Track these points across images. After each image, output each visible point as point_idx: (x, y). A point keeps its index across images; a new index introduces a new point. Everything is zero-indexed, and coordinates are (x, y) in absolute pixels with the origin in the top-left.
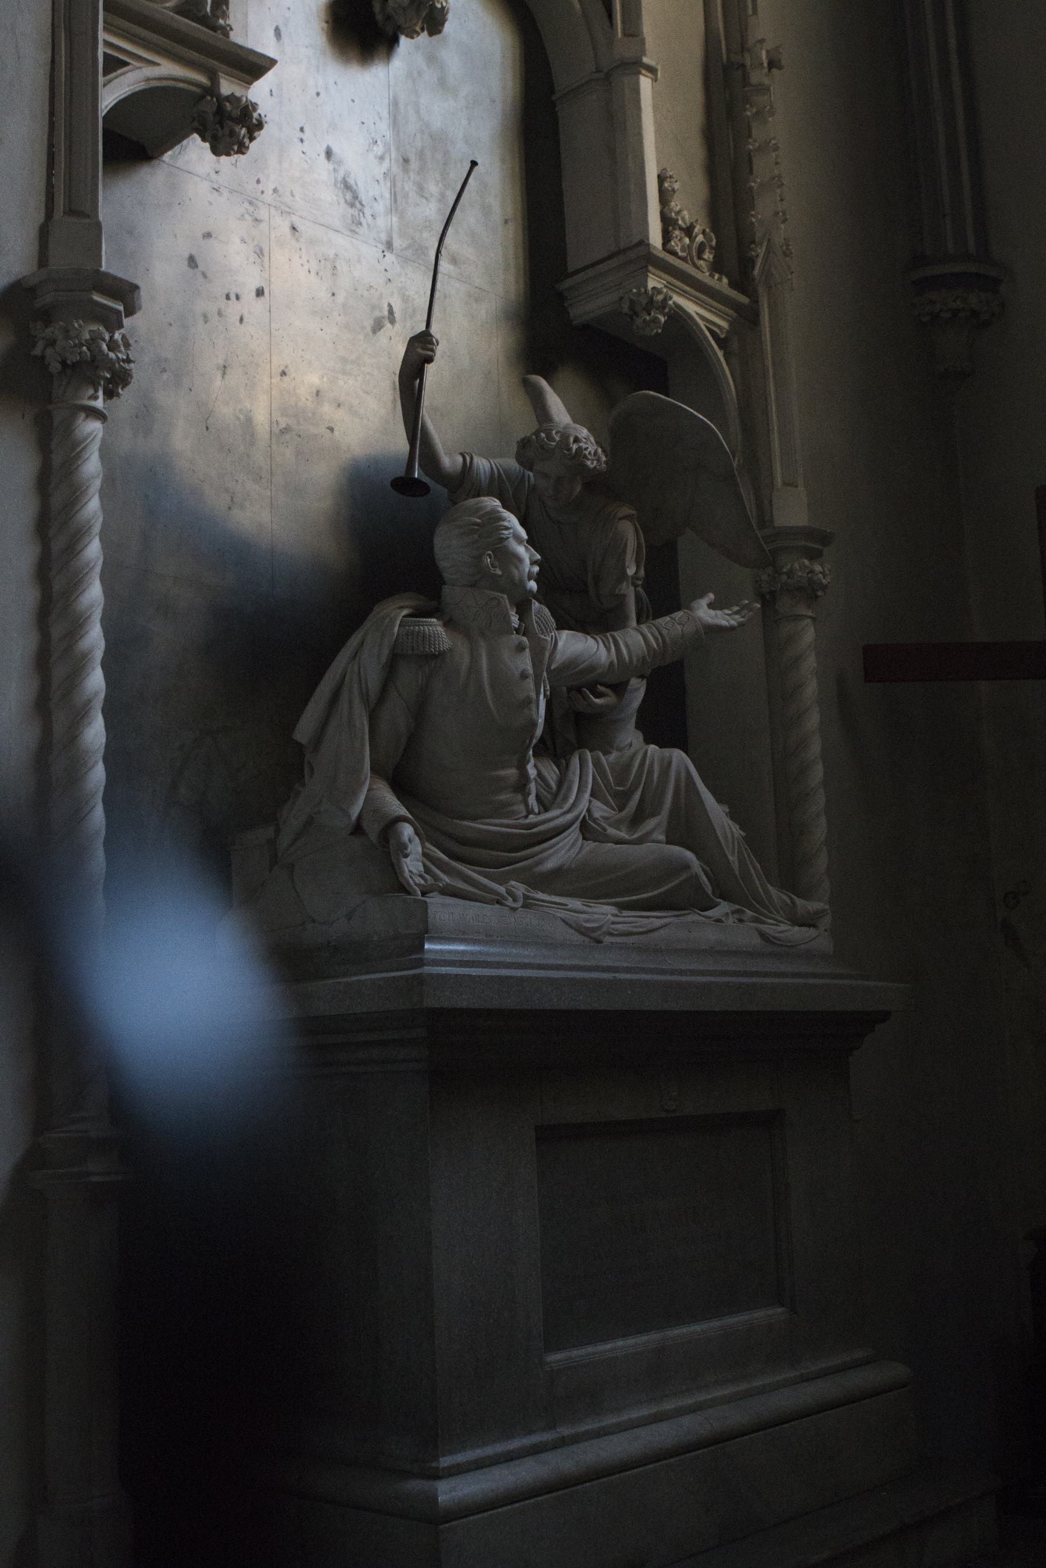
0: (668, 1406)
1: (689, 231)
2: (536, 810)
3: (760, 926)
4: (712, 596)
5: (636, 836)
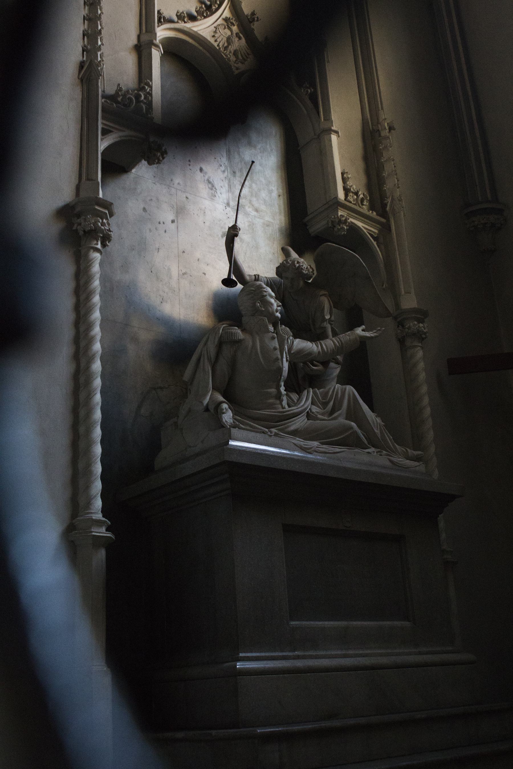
0: (351, 652)
1: (356, 194)
3: (390, 458)
4: (364, 327)
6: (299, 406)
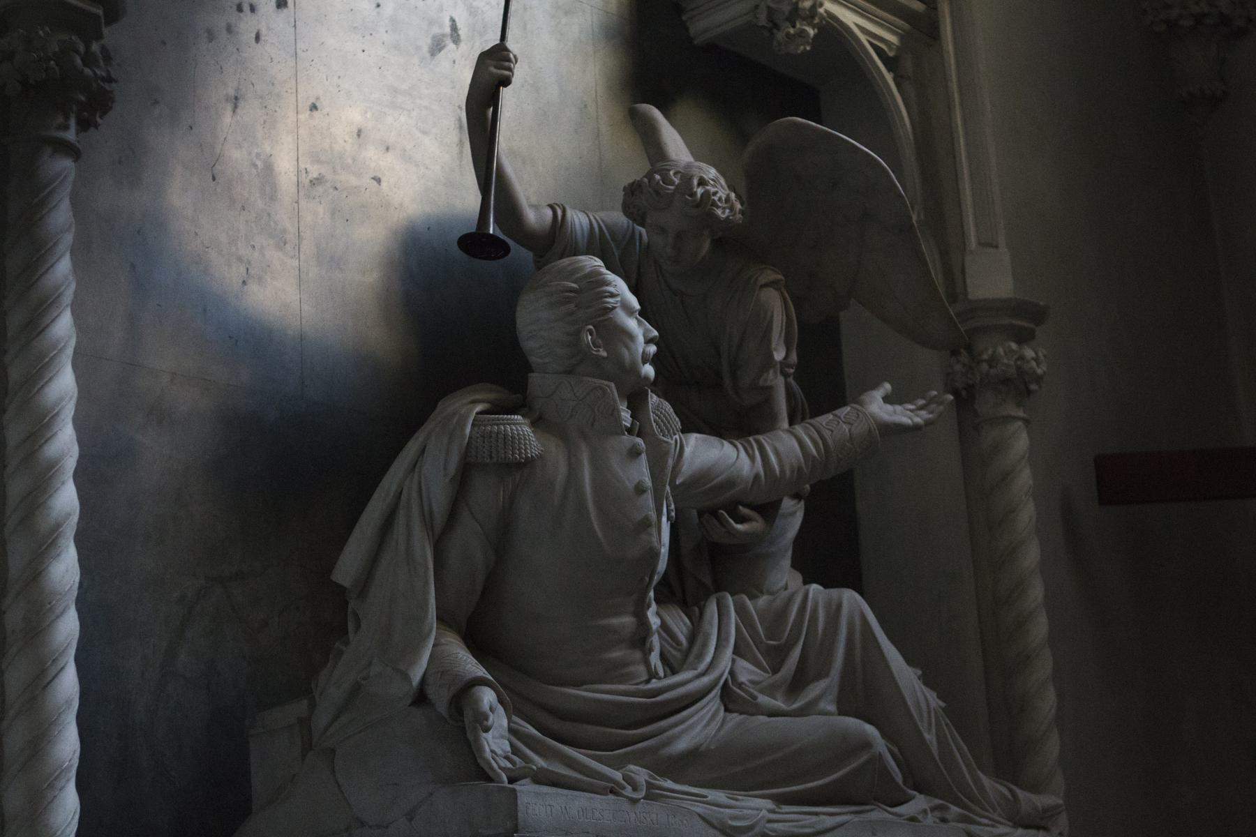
2: (661, 674)
3: (973, 828)
4: (888, 386)
5: (795, 706)
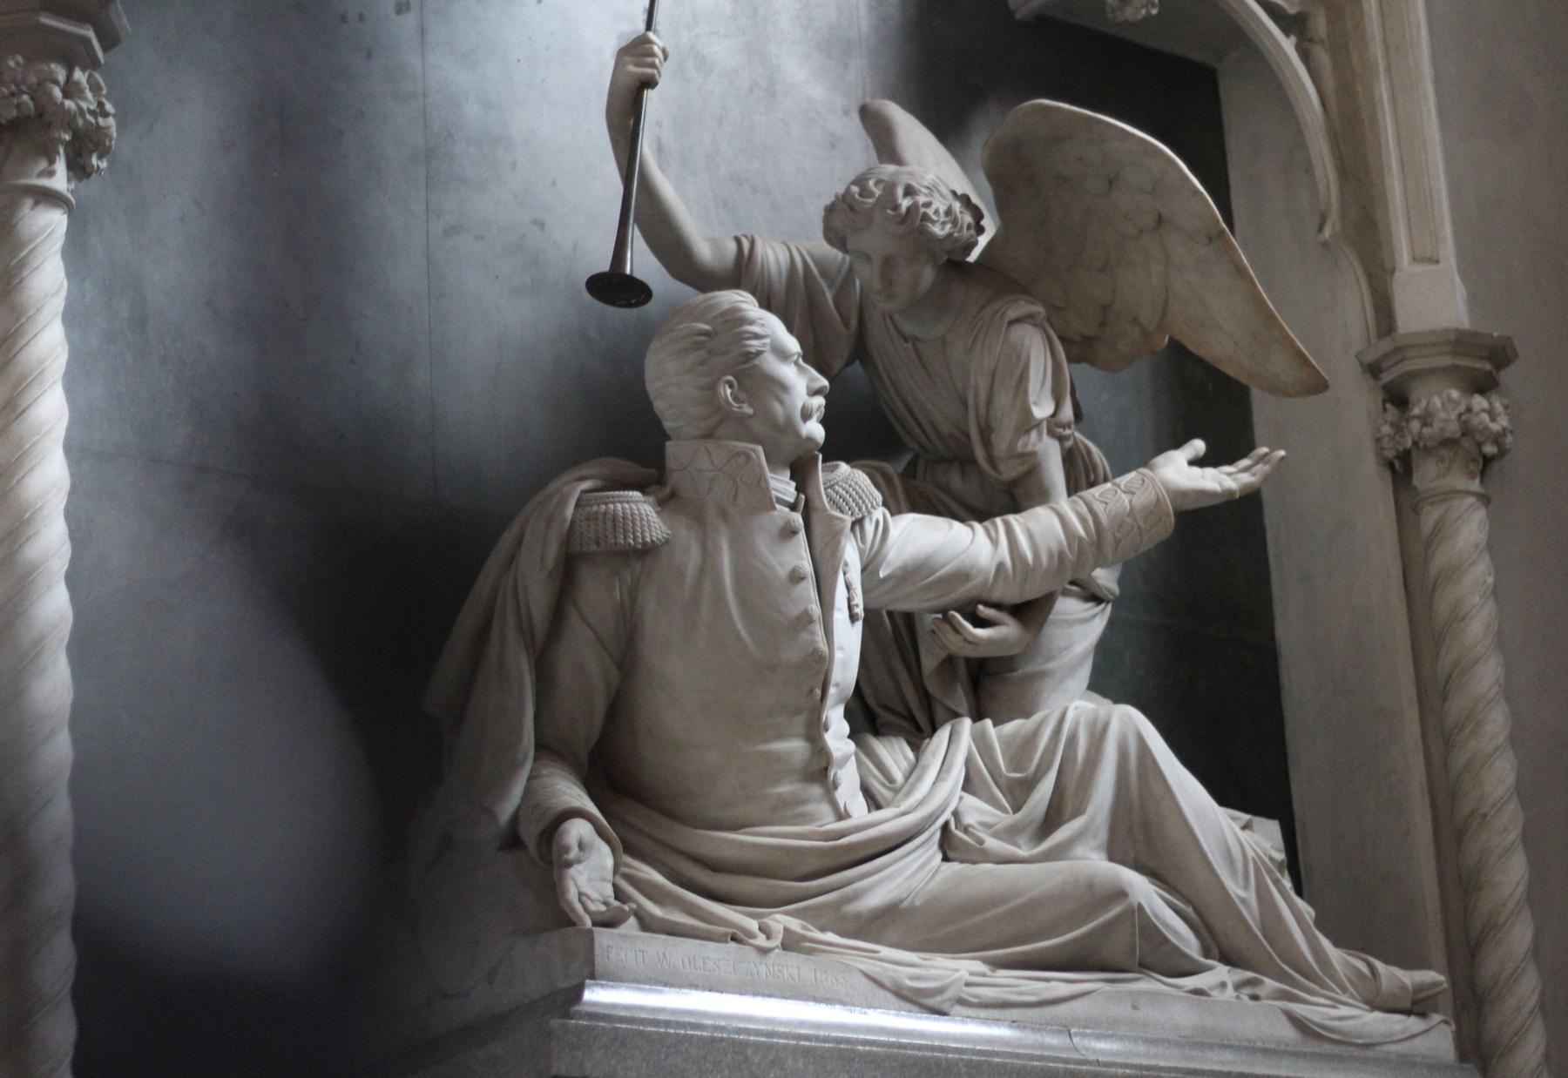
6: (905, 806)
